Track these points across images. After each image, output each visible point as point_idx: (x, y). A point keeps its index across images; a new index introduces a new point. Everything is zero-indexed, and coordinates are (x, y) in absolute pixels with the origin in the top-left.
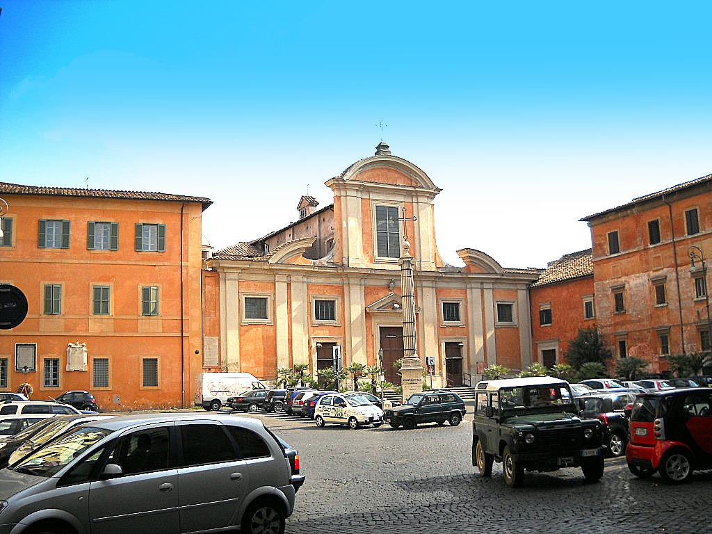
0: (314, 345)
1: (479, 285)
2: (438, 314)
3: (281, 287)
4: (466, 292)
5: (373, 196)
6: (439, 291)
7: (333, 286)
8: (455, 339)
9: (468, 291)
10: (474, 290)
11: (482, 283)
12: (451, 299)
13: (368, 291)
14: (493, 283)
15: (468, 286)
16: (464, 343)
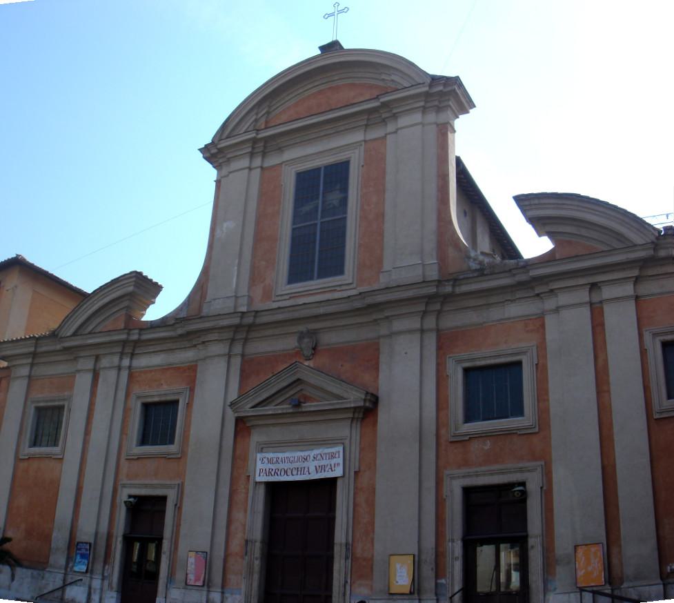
0: (124, 495)
1: (584, 295)
2: (441, 403)
3: (83, 382)
4: (543, 326)
5: (289, 155)
6: (445, 342)
7: (179, 368)
8: (502, 472)
9: (550, 321)
10: (565, 314)
11: (594, 286)
12: (486, 353)
13: (249, 369)
14: (637, 280)
15: (550, 304)
16: (533, 487)
